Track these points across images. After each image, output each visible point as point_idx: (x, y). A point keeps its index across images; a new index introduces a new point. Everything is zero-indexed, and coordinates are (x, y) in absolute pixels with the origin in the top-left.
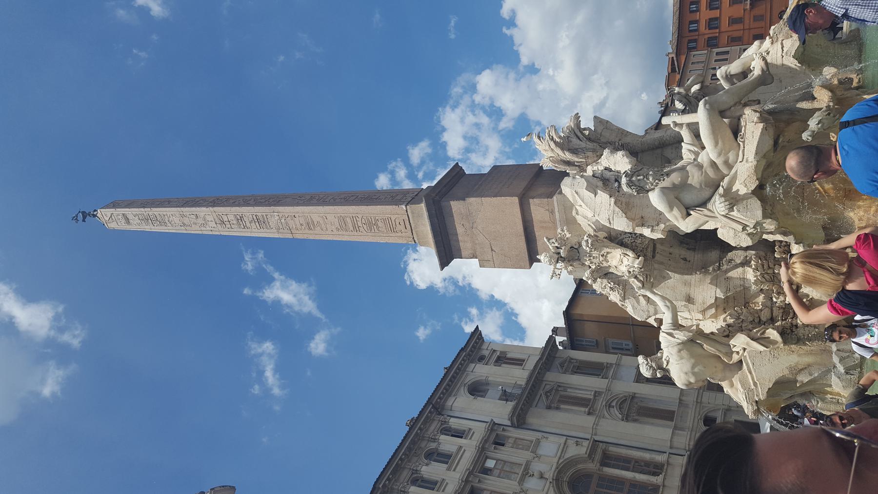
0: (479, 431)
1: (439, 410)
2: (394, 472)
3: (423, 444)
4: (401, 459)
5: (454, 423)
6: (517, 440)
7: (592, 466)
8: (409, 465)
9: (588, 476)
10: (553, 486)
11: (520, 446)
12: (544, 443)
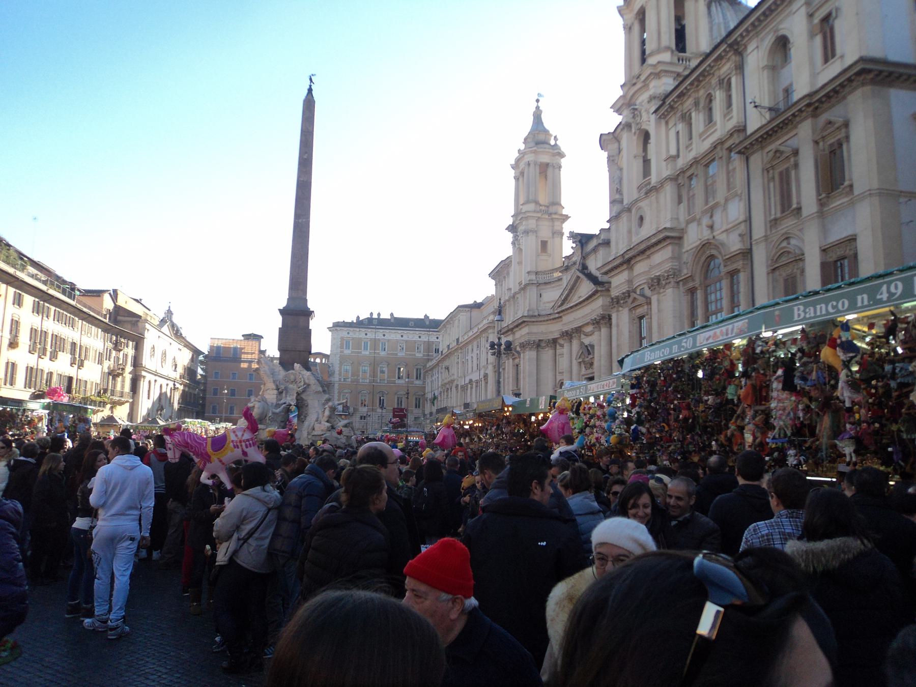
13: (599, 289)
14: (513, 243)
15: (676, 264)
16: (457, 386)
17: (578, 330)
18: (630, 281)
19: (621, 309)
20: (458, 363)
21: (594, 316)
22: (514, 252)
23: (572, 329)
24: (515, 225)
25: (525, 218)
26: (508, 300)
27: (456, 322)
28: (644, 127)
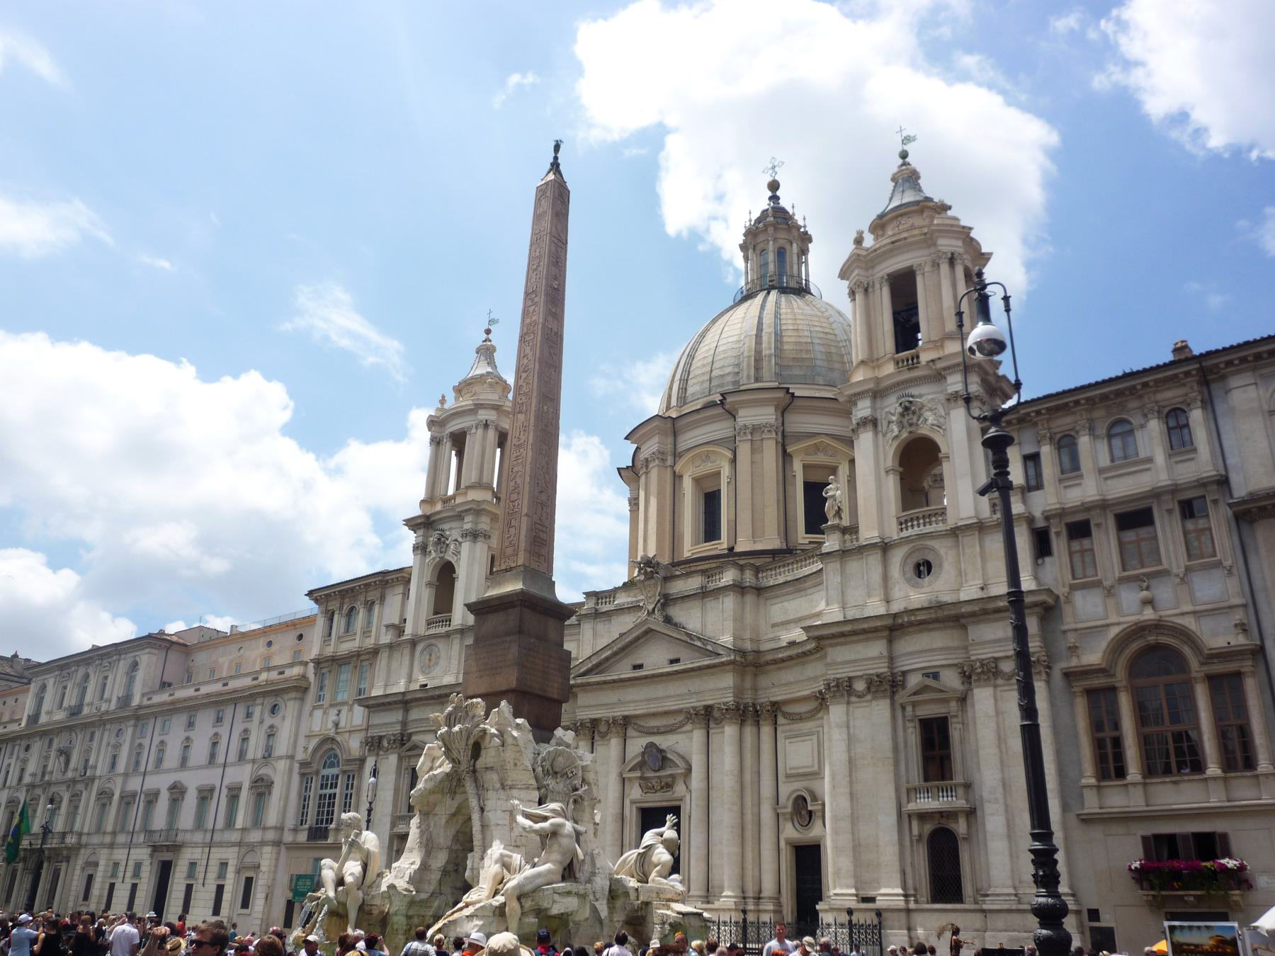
0: (1202, 464)
1: (1211, 377)
2: (1058, 409)
3: (1133, 404)
4: (1077, 403)
5: (1196, 416)
6: (1207, 532)
7: (1194, 664)
8: (1081, 415)
9: (1183, 665)
10: (1129, 627)
11: (1196, 544)
12: (1217, 574)
13: (738, 659)
14: (421, 549)
15: (1038, 644)
16: (105, 796)
17: (625, 723)
18: (891, 659)
19: (853, 699)
20: (117, 746)
21: (697, 702)
22: (422, 564)
23: (614, 718)
24: (433, 519)
25: (475, 510)
26: (391, 646)
27: (123, 666)
28: (924, 431)
